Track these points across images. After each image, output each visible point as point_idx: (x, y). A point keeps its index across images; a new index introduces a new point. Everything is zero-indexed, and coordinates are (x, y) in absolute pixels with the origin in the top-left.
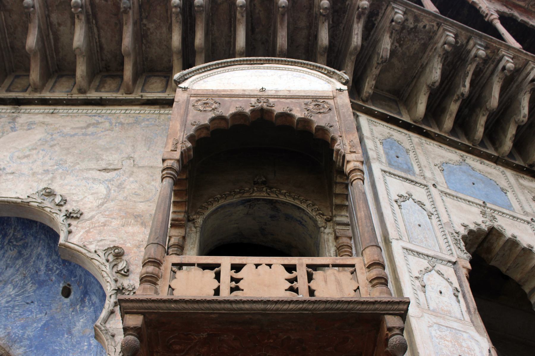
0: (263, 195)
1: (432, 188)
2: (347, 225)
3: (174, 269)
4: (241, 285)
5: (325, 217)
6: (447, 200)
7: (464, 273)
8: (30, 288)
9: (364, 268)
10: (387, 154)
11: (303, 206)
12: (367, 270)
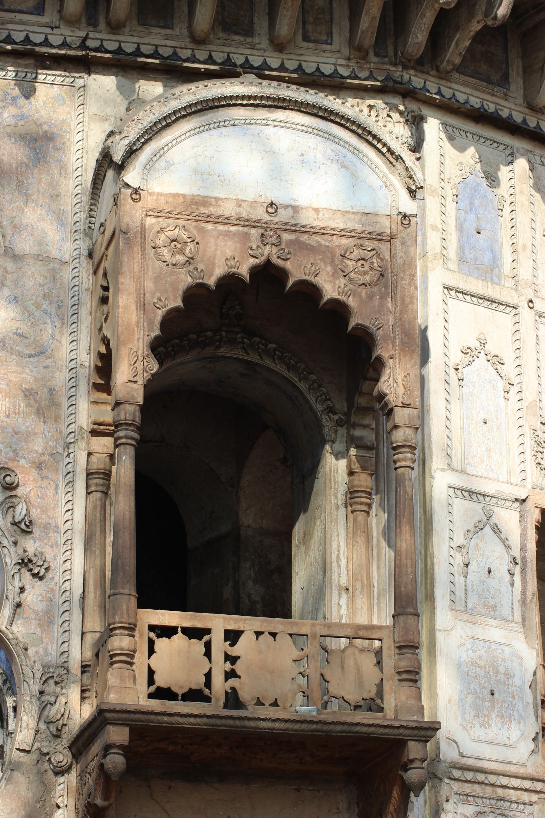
0: (238, 353)
1: (524, 311)
2: (369, 448)
3: (152, 635)
4: (239, 667)
5: (336, 417)
9: (393, 647)
10: (460, 228)
11: (303, 387)
12: (397, 651)
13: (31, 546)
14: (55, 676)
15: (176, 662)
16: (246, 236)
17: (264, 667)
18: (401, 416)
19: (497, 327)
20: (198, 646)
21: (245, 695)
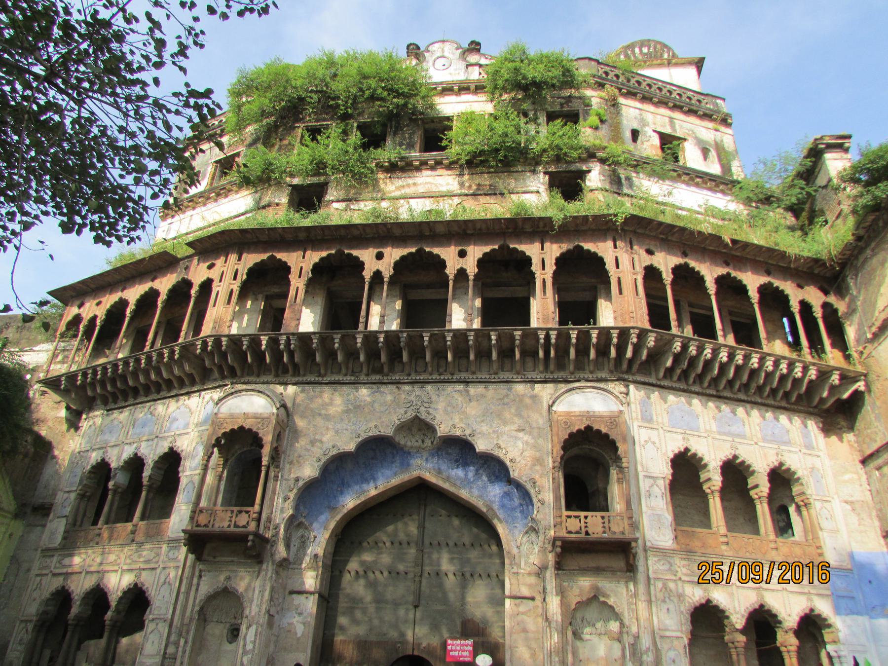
6: (667, 434)
7: (667, 482)
8: (493, 478)
10: (641, 411)
13: (540, 497)
14: (547, 528)
15: (574, 524)
16: (582, 420)
17: (594, 524)
18: (624, 460)
19: (653, 434)
20: (578, 520)
21: (590, 532)
